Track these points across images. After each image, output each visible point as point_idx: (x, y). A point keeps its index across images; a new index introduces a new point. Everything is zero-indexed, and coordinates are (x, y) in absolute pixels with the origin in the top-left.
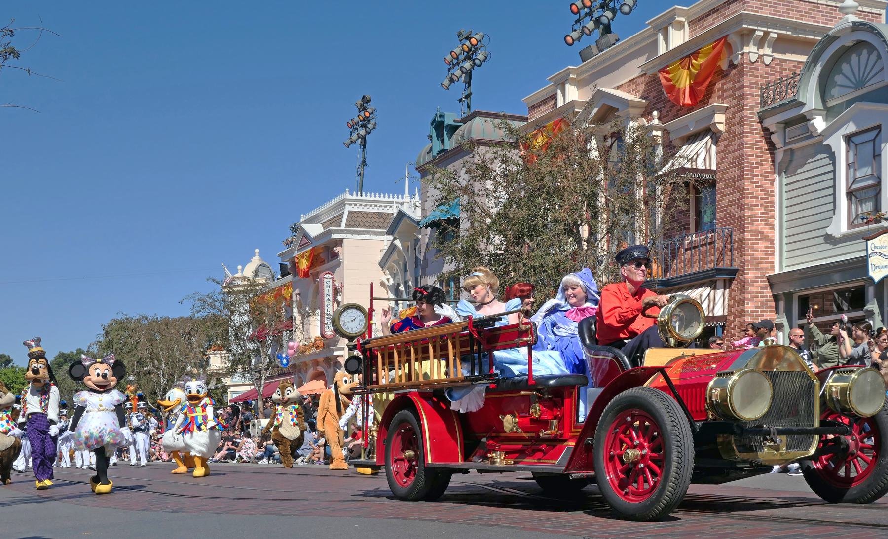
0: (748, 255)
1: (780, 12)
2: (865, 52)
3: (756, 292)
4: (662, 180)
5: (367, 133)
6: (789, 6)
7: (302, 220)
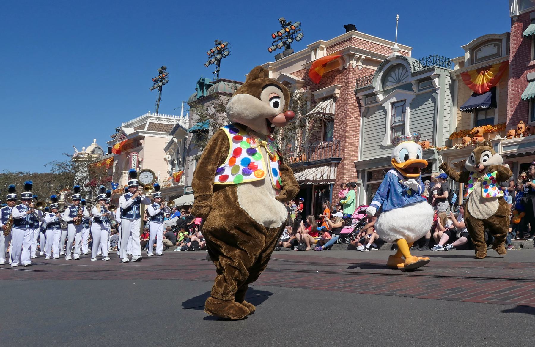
0: (347, 152)
1: (367, 47)
2: (401, 68)
3: (349, 169)
4: (310, 117)
5: (163, 84)
6: (371, 45)
7: (123, 125)
